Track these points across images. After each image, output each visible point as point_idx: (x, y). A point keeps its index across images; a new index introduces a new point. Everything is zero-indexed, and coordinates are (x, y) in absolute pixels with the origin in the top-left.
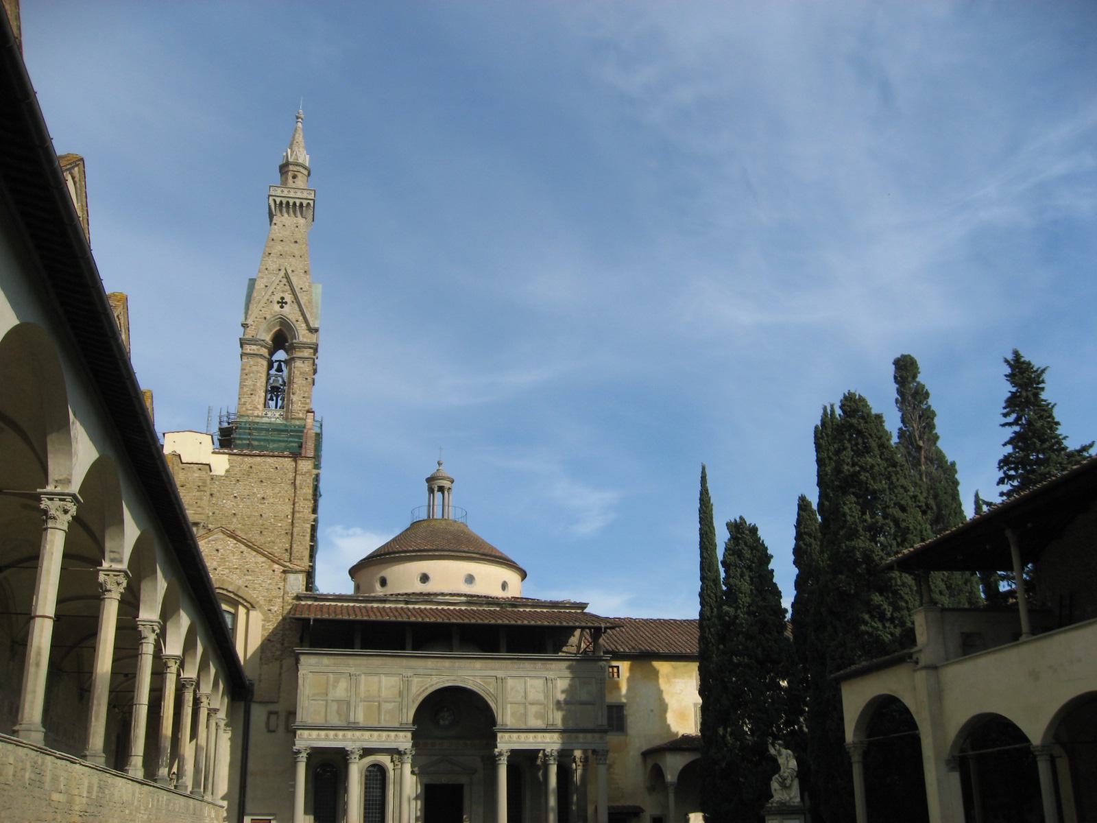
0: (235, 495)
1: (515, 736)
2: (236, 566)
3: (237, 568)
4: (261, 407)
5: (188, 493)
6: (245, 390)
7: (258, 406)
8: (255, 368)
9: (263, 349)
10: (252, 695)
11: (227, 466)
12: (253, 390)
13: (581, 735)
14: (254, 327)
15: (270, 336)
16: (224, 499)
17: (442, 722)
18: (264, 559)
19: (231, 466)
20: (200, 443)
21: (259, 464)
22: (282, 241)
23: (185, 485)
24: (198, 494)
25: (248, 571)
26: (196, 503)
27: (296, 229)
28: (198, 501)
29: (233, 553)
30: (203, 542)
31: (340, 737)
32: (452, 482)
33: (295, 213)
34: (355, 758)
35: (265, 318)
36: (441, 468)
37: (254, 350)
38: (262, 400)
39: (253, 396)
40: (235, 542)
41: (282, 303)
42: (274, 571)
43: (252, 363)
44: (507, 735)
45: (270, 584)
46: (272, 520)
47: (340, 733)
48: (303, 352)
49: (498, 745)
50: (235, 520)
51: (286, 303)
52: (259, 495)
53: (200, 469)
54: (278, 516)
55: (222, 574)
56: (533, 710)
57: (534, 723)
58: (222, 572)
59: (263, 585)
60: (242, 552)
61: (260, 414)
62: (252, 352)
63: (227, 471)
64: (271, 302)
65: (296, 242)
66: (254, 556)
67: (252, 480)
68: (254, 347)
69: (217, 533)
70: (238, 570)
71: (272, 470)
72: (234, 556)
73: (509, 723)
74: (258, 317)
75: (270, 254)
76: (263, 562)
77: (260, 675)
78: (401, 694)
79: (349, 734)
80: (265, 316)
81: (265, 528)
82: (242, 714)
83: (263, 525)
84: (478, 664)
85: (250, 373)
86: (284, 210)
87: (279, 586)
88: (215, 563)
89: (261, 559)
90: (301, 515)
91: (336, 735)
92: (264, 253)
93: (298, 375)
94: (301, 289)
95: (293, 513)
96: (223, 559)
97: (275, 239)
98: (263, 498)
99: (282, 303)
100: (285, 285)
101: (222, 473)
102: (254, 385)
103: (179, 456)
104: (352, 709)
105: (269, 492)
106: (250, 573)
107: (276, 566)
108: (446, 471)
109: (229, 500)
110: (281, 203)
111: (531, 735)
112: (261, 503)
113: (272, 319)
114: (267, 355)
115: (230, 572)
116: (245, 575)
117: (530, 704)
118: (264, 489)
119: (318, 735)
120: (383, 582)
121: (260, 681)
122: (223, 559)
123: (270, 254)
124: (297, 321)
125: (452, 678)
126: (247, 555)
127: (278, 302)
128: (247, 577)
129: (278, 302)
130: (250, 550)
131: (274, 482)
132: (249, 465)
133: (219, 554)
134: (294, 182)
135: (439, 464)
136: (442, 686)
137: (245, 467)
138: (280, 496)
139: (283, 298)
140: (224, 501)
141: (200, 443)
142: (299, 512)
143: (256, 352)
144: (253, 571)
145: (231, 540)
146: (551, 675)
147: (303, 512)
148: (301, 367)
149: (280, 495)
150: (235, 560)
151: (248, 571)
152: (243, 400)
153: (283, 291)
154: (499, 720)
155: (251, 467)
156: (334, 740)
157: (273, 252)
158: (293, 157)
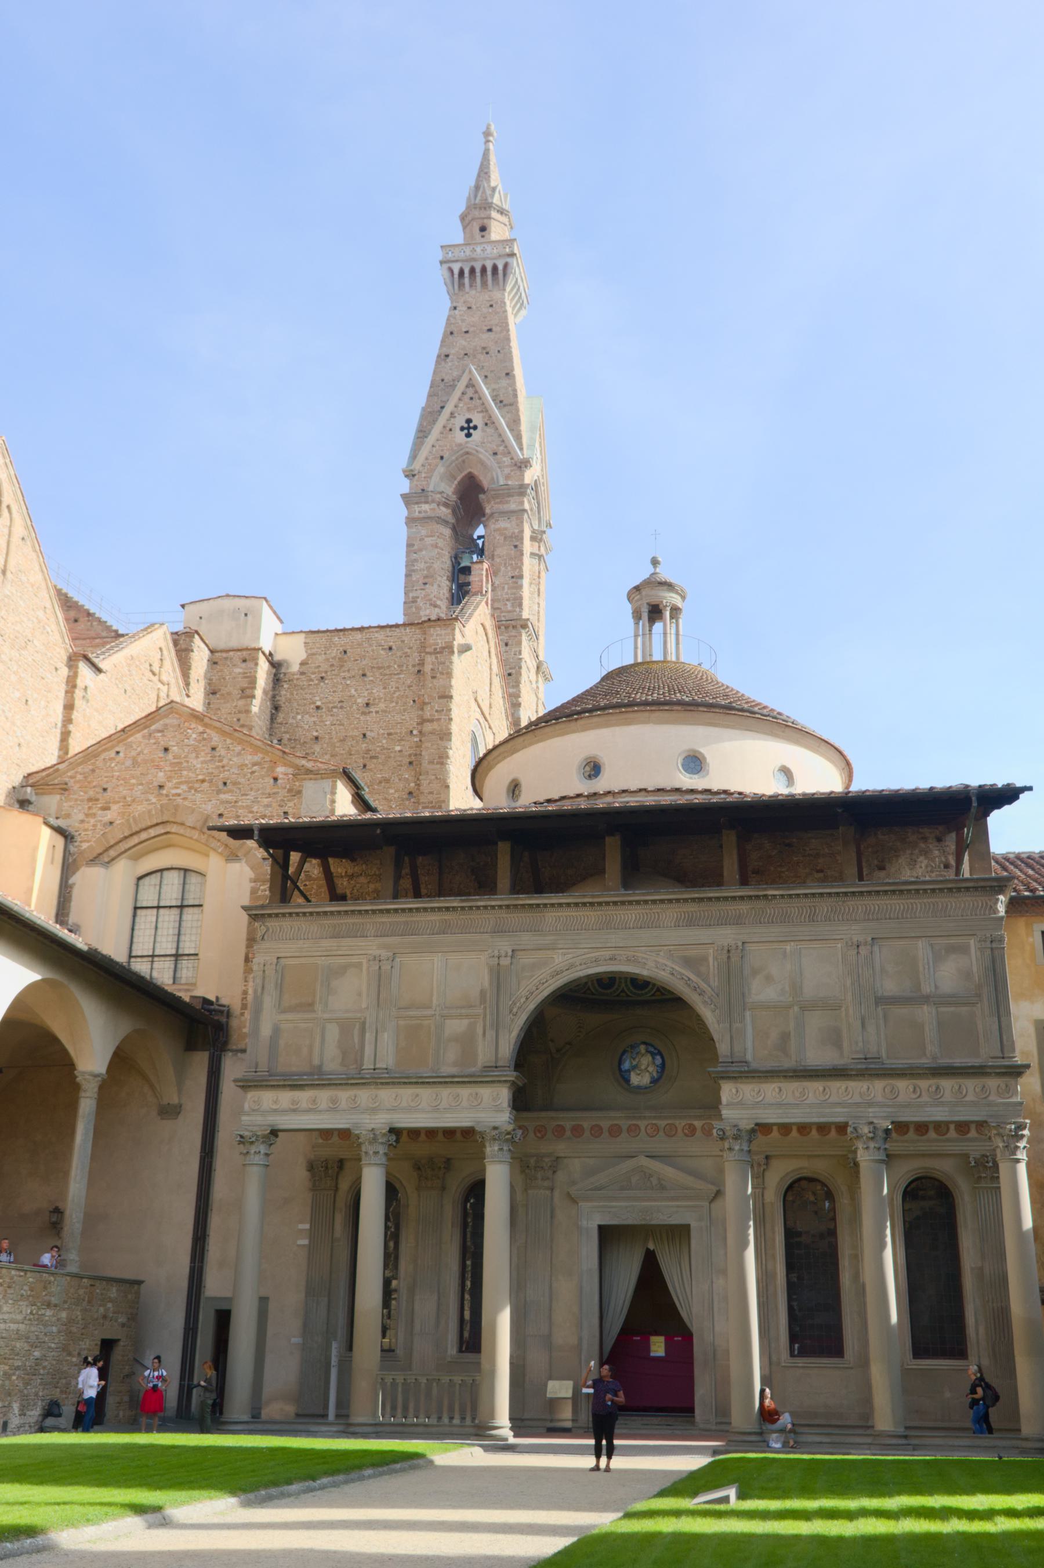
0: (318, 703)
1: (770, 1090)
2: (200, 777)
3: (203, 781)
4: (443, 604)
5: (225, 703)
6: (414, 579)
7: (439, 603)
8: (429, 541)
9: (443, 509)
10: (227, 1036)
11: (303, 656)
12: (426, 577)
13: (947, 1084)
14: (423, 475)
15: (454, 486)
16: (298, 713)
17: (635, 1079)
18: (257, 758)
19: (311, 655)
20: (246, 615)
21: (360, 645)
22: (467, 332)
23: (220, 690)
24: (241, 703)
25: (225, 784)
26: (239, 720)
27: (490, 310)
28: (242, 716)
29: (196, 750)
30: (139, 736)
31: (343, 1104)
32: (683, 598)
33: (484, 283)
34: (376, 1153)
35: (442, 458)
36: (658, 570)
37: (426, 512)
38: (445, 593)
39: (427, 586)
40: (201, 729)
41: (469, 428)
42: (276, 779)
43: (424, 532)
44: (748, 1090)
45: (268, 806)
46: (384, 741)
47: (344, 1095)
48: (507, 502)
49: (725, 1112)
50: (317, 748)
51: (475, 428)
52: (359, 700)
53: (244, 661)
54: (396, 733)
55: (174, 795)
56: (815, 1022)
57: (817, 1056)
58: (174, 791)
59: (255, 809)
60: (213, 749)
61: (443, 616)
62: (422, 515)
63: (302, 664)
64: (451, 430)
65: (490, 330)
66: (239, 754)
67: (347, 674)
68: (425, 507)
69: (166, 716)
70: (206, 784)
71: (382, 652)
72: (197, 757)
73: (749, 1057)
74: (430, 458)
75: (447, 356)
76: (254, 764)
77: (245, 993)
78: (483, 993)
79: (364, 1096)
80: (442, 454)
81: (372, 758)
82: (203, 1080)
83: (368, 751)
84: (670, 914)
85: (420, 550)
86: (467, 280)
87: (286, 809)
88: (161, 774)
89: (249, 759)
90: (435, 726)
91: (334, 1101)
92: (439, 356)
93: (502, 541)
94: (501, 402)
95: (423, 721)
96: (178, 766)
97: (455, 330)
98: (367, 704)
99: (469, 428)
100: (471, 399)
101: (295, 668)
102: (428, 568)
103: (197, 632)
104: (369, 1036)
105: (378, 691)
106: (229, 786)
107: (280, 770)
108: (665, 573)
109: (307, 713)
110: (461, 272)
111: (814, 1089)
112: (364, 713)
113: (454, 458)
114: (451, 520)
115: (190, 788)
116: (219, 792)
117: (803, 1009)
118: (368, 687)
119: (294, 1102)
120: (514, 788)
121: (244, 1007)
122: (178, 766)
123: (447, 356)
124: (495, 454)
125: (608, 954)
126: (223, 752)
127: (462, 429)
128: (222, 796)
129: (462, 429)
130: (229, 741)
131: (387, 672)
132: (341, 649)
133: (170, 756)
134: (483, 236)
135: (655, 562)
136: (582, 974)
137: (334, 652)
138: (398, 698)
139: (469, 421)
140: (299, 717)
141: (246, 615)
142: (431, 721)
143: (430, 514)
144: (235, 784)
145: (193, 726)
146: (856, 932)
147: (439, 720)
148: (506, 529)
149: (397, 694)
150: (199, 764)
151: (225, 784)
152: (411, 595)
153: (469, 410)
154: (723, 1048)
155: (345, 652)
156: (333, 1110)
157: (452, 351)
158: (479, 198)
